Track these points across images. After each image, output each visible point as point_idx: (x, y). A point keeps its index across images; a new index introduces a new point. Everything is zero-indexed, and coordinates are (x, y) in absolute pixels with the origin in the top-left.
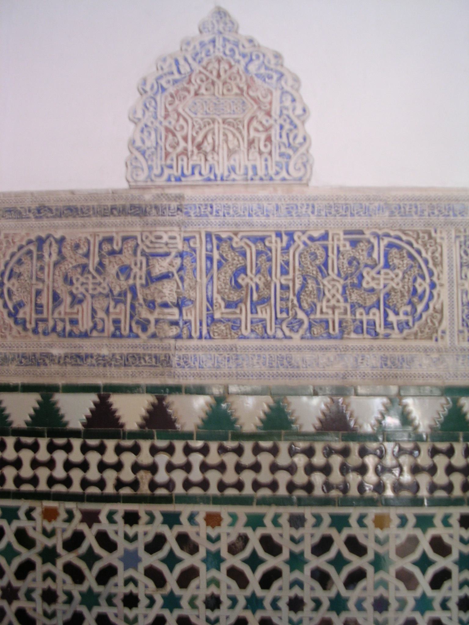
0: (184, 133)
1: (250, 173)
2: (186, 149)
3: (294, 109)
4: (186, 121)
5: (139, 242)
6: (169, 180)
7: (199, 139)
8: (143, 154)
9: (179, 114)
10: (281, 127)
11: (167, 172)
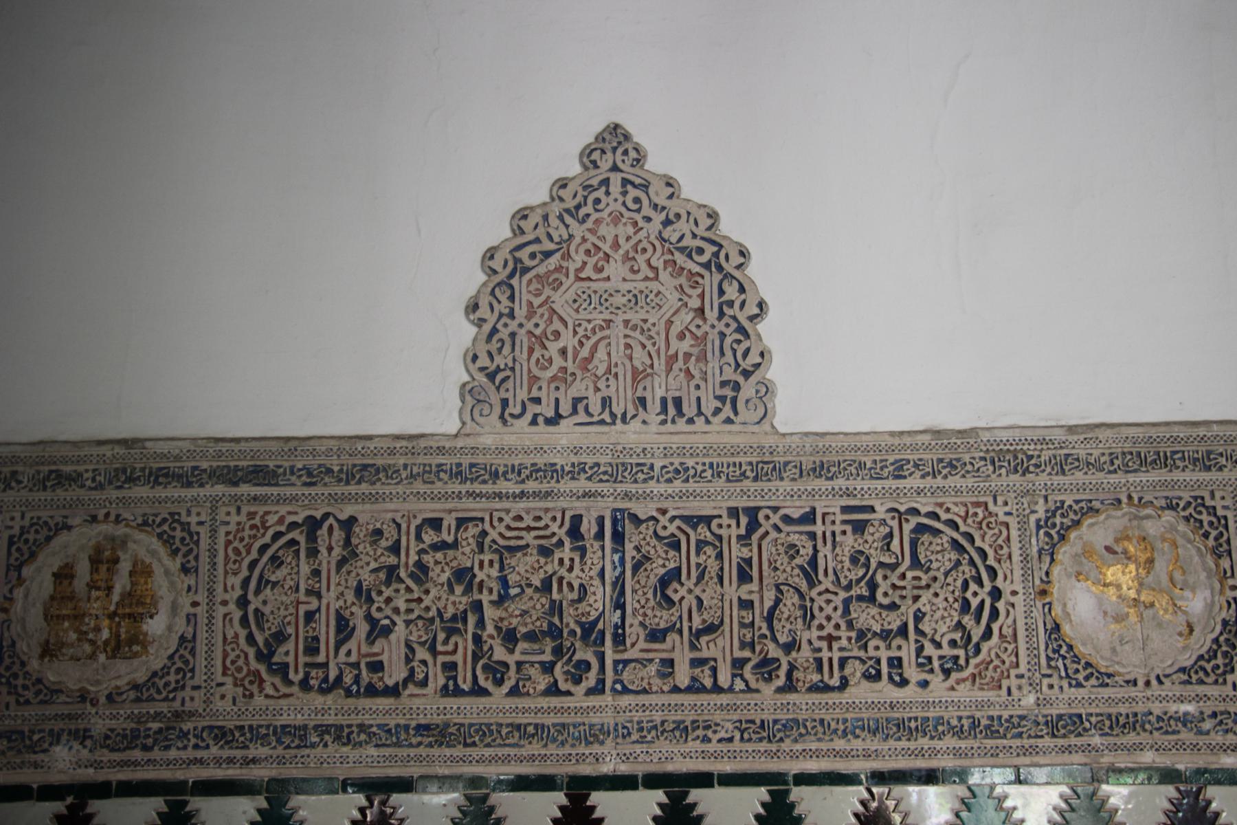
0: (561, 344)
3: (743, 304)
4: (565, 324)
5: (487, 526)
7: (585, 353)
8: (491, 377)
10: (722, 335)
11: (532, 409)
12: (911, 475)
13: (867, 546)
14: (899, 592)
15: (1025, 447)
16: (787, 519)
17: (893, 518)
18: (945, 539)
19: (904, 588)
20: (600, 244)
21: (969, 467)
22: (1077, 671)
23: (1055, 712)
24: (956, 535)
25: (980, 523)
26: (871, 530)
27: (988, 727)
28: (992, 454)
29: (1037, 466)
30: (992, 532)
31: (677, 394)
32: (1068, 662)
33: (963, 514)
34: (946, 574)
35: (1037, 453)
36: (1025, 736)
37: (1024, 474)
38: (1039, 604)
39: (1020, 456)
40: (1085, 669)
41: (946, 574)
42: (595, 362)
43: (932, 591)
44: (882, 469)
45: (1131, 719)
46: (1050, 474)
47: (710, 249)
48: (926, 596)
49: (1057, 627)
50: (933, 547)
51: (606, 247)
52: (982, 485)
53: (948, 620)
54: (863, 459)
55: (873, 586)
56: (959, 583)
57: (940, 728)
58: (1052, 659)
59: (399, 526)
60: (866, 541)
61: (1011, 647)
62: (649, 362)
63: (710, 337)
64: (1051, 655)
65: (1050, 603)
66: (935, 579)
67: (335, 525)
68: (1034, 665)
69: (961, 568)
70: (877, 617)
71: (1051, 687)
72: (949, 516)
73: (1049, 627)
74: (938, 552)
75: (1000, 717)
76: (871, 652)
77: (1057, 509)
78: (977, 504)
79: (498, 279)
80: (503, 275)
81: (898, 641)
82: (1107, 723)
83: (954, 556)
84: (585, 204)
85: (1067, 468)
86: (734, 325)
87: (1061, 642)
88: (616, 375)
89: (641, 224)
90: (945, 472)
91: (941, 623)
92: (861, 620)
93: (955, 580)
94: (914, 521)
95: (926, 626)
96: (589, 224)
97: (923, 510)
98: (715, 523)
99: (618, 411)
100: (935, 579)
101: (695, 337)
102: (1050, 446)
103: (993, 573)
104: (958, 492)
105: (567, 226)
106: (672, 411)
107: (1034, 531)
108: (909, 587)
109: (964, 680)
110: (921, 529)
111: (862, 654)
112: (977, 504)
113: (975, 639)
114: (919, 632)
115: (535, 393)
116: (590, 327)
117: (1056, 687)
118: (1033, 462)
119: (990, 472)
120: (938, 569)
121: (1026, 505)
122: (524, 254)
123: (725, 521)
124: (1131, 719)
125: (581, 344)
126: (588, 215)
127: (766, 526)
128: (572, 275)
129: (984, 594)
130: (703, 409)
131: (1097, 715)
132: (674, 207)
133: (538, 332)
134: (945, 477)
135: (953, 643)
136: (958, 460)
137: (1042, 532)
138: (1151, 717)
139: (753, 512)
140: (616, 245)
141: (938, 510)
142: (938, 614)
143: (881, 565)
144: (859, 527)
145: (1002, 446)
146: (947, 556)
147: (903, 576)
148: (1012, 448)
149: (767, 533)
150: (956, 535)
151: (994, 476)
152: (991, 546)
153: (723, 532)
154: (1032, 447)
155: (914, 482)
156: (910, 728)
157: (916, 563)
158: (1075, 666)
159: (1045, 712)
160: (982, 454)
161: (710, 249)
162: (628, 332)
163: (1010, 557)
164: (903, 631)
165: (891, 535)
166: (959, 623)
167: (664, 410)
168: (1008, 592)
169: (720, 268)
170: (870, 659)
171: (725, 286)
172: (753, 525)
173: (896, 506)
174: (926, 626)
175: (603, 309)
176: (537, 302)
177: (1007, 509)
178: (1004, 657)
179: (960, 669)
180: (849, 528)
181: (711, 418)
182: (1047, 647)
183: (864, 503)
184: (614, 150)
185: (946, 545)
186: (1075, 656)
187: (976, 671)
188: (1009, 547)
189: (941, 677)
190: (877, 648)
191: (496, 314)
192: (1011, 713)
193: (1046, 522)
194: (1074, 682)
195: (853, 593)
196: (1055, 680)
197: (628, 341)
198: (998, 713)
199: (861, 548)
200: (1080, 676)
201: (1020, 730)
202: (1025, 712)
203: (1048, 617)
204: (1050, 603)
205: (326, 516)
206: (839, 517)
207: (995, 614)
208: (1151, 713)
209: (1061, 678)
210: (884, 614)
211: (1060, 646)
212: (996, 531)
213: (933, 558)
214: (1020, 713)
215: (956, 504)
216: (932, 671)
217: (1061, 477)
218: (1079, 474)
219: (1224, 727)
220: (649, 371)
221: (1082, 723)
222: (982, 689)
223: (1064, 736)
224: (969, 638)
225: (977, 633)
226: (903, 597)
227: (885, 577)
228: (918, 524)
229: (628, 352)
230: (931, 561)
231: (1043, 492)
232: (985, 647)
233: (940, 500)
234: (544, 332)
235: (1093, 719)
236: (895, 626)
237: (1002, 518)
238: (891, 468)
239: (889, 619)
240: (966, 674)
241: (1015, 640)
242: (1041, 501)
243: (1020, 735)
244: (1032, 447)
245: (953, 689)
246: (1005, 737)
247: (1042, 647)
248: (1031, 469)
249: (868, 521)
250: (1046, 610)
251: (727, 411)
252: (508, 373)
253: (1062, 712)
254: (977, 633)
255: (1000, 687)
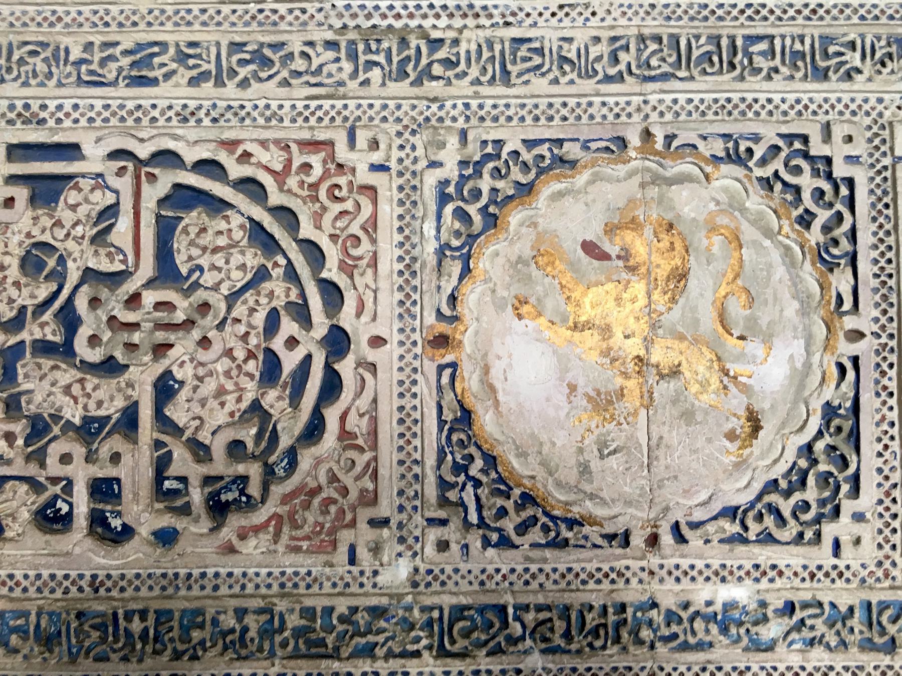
12: (168, 76)
13: (60, 233)
14: (125, 336)
15: (427, 23)
17: (121, 171)
18: (236, 220)
19: (135, 326)
21: (299, 64)
22: (502, 512)
23: (447, 601)
24: (259, 213)
25: (315, 186)
26: (73, 197)
27: (298, 633)
28: (352, 35)
29: (449, 63)
30: (337, 208)
32: (483, 492)
33: (278, 167)
34: (233, 298)
35: (451, 34)
36: (380, 652)
37: (418, 82)
38: (430, 368)
39: (413, 43)
40: (519, 507)
41: (233, 298)
43: (196, 334)
44: (103, 62)
45: (612, 618)
46: (477, 82)
48: (183, 347)
49: (466, 416)
50: (207, 239)
52: (326, 104)
53: (230, 398)
54: (65, 41)
55: (69, 320)
56: (259, 319)
57: (196, 635)
58: (453, 486)
60: (58, 224)
64: (451, 479)
65: (454, 365)
66: (205, 307)
68: (409, 500)
69: (267, 286)
70: (76, 389)
71: (443, 546)
72: (247, 171)
73: (448, 416)
74: (216, 250)
75: (329, 611)
76: (54, 467)
77: (488, 157)
78: (313, 145)
81: (116, 443)
82: (560, 626)
83: (253, 259)
85: (513, 69)
87: (473, 450)
90: (243, 72)
91: (213, 403)
92: (38, 398)
93: (252, 311)
94: (167, 179)
95: (178, 413)
97: (191, 156)
100: (205, 307)
102: (483, 21)
103: (332, 294)
104: (273, 118)
107: (433, 207)
108: (147, 326)
109: (257, 529)
110: (184, 197)
111: (32, 470)
112: (313, 145)
113: (285, 442)
114: (162, 420)
117: (455, 547)
118: (441, 54)
119: (344, 76)
120: (216, 288)
121: (420, 152)
124: (612, 618)
131: (539, 608)
134: (244, 84)
136: (277, 46)
137: (449, 209)
138: (654, 613)
141: (223, 157)
142: (210, 386)
143: (89, 274)
144: (46, 191)
145: (376, 20)
146: (237, 259)
147: (134, 300)
148: (398, 24)
150: (259, 213)
151: (353, 85)
152: (334, 237)
154: (443, 22)
155: (174, 92)
156: (128, 633)
157: (166, 271)
158: (500, 502)
159: (428, 601)
160: (330, 36)
163: (374, 263)
164: (129, 421)
165: (111, 211)
166: (256, 405)
168: (364, 339)
170: (55, 480)
173: (131, 145)
174: (178, 413)
177: (376, 157)
178: (347, 480)
179: (250, 505)
180: (22, 194)
182: (441, 460)
183: (58, 138)
185: (238, 235)
186: (501, 480)
187: (283, 510)
188: (374, 241)
189: (205, 525)
190: (66, 459)
192: (354, 602)
193: (459, 187)
194: (495, 537)
195: (25, 336)
196: (451, 533)
198: (327, 602)
199: (47, 238)
200: (509, 525)
201: (371, 638)
202: (385, 601)
203: (449, 396)
204: (454, 365)
207: (332, 385)
208: (655, 605)
209: (467, 525)
210: (91, 381)
211: (471, 458)
212: (349, 205)
213: (204, 262)
214: (374, 601)
215: (263, 144)
216: (185, 510)
217: (500, 90)
218: (540, 84)
219: (807, 634)
221: (505, 624)
222: (297, 550)
223: (462, 655)
224: (275, 437)
225: (289, 430)
226: (131, 347)
227: (95, 302)
228: (177, 186)
230: (200, 268)
231: (461, 123)
232: (306, 459)
233: (229, 135)
235: (530, 617)
236: (113, 408)
237: (364, 176)
238: (126, 61)
239: (100, 394)
240: (260, 516)
241: (375, 447)
242: (453, 141)
243: (369, 652)
244: (443, 22)
245: (230, 549)
246: (335, 655)
247: (431, 461)
248: (437, 70)
249: (70, 177)
250: (445, 380)
253: (464, 600)
254: (289, 430)
255: (334, 544)
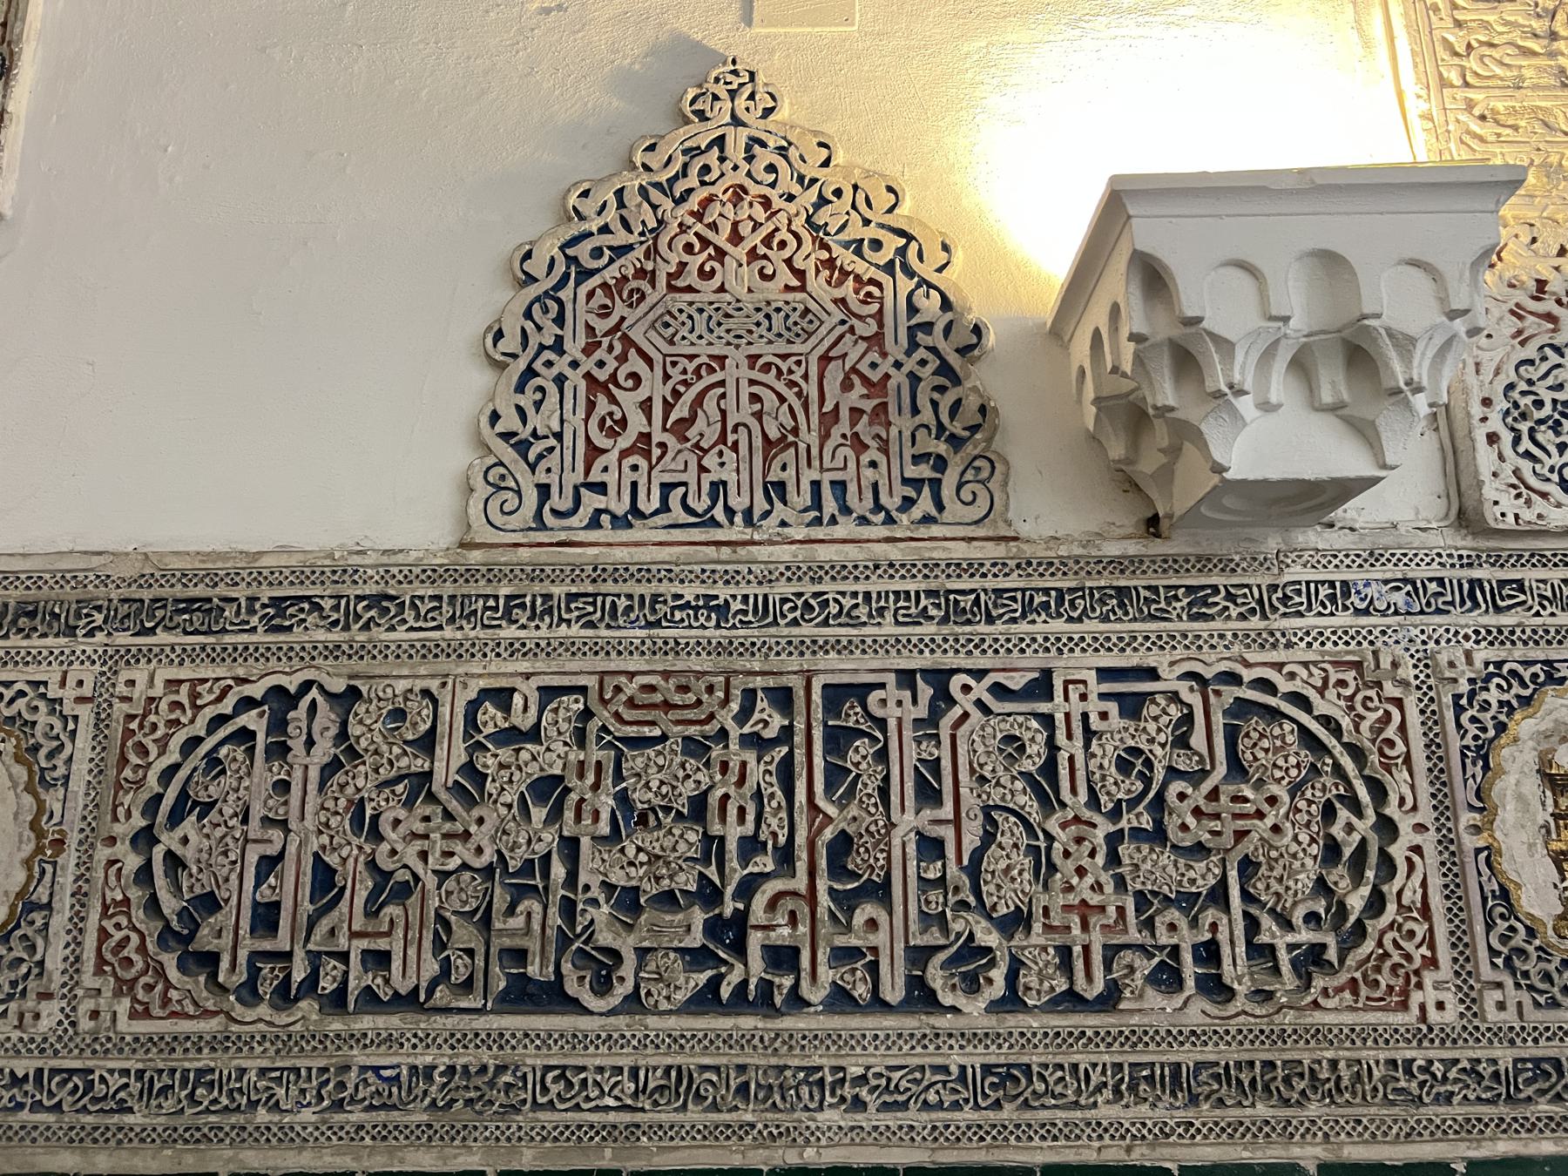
0: (643, 393)
1: (830, 506)
2: (646, 437)
4: (649, 361)
6: (594, 523)
8: (522, 448)
9: (627, 341)
10: (914, 379)
11: (592, 501)
16: (999, 691)
20: (710, 235)
31: (838, 476)
42: (700, 423)
47: (893, 243)
51: (721, 239)
59: (435, 702)
61: (1420, 930)
62: (790, 423)
63: (892, 384)
67: (320, 699)
79: (534, 291)
80: (548, 284)
84: (685, 175)
86: (934, 363)
88: (735, 447)
89: (777, 203)
96: (693, 203)
98: (874, 697)
99: (738, 502)
101: (865, 380)
105: (655, 207)
106: (830, 506)
115: (595, 477)
116: (691, 367)
122: (583, 251)
123: (893, 692)
125: (677, 394)
126: (690, 191)
127: (965, 702)
128: (662, 281)
129: (1365, 826)
130: (884, 499)
132: (831, 179)
133: (602, 375)
135: (1312, 918)
139: (938, 678)
140: (736, 238)
149: (966, 715)
153: (892, 713)
157: (1237, 769)
161: (893, 243)
162: (756, 375)
167: (817, 503)
169: (910, 273)
171: (920, 300)
172: (943, 698)
175: (712, 338)
176: (602, 326)
180: (1113, 708)
181: (894, 514)
184: (733, 94)
191: (531, 351)
197: (756, 389)
205: (307, 686)
206: (1095, 688)
220: (791, 438)
225: (1356, 902)
229: (757, 407)
234: (613, 377)
251: (925, 504)
252: (552, 442)
254: (1356, 902)
